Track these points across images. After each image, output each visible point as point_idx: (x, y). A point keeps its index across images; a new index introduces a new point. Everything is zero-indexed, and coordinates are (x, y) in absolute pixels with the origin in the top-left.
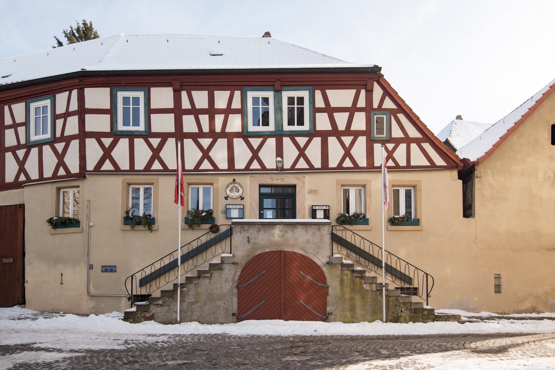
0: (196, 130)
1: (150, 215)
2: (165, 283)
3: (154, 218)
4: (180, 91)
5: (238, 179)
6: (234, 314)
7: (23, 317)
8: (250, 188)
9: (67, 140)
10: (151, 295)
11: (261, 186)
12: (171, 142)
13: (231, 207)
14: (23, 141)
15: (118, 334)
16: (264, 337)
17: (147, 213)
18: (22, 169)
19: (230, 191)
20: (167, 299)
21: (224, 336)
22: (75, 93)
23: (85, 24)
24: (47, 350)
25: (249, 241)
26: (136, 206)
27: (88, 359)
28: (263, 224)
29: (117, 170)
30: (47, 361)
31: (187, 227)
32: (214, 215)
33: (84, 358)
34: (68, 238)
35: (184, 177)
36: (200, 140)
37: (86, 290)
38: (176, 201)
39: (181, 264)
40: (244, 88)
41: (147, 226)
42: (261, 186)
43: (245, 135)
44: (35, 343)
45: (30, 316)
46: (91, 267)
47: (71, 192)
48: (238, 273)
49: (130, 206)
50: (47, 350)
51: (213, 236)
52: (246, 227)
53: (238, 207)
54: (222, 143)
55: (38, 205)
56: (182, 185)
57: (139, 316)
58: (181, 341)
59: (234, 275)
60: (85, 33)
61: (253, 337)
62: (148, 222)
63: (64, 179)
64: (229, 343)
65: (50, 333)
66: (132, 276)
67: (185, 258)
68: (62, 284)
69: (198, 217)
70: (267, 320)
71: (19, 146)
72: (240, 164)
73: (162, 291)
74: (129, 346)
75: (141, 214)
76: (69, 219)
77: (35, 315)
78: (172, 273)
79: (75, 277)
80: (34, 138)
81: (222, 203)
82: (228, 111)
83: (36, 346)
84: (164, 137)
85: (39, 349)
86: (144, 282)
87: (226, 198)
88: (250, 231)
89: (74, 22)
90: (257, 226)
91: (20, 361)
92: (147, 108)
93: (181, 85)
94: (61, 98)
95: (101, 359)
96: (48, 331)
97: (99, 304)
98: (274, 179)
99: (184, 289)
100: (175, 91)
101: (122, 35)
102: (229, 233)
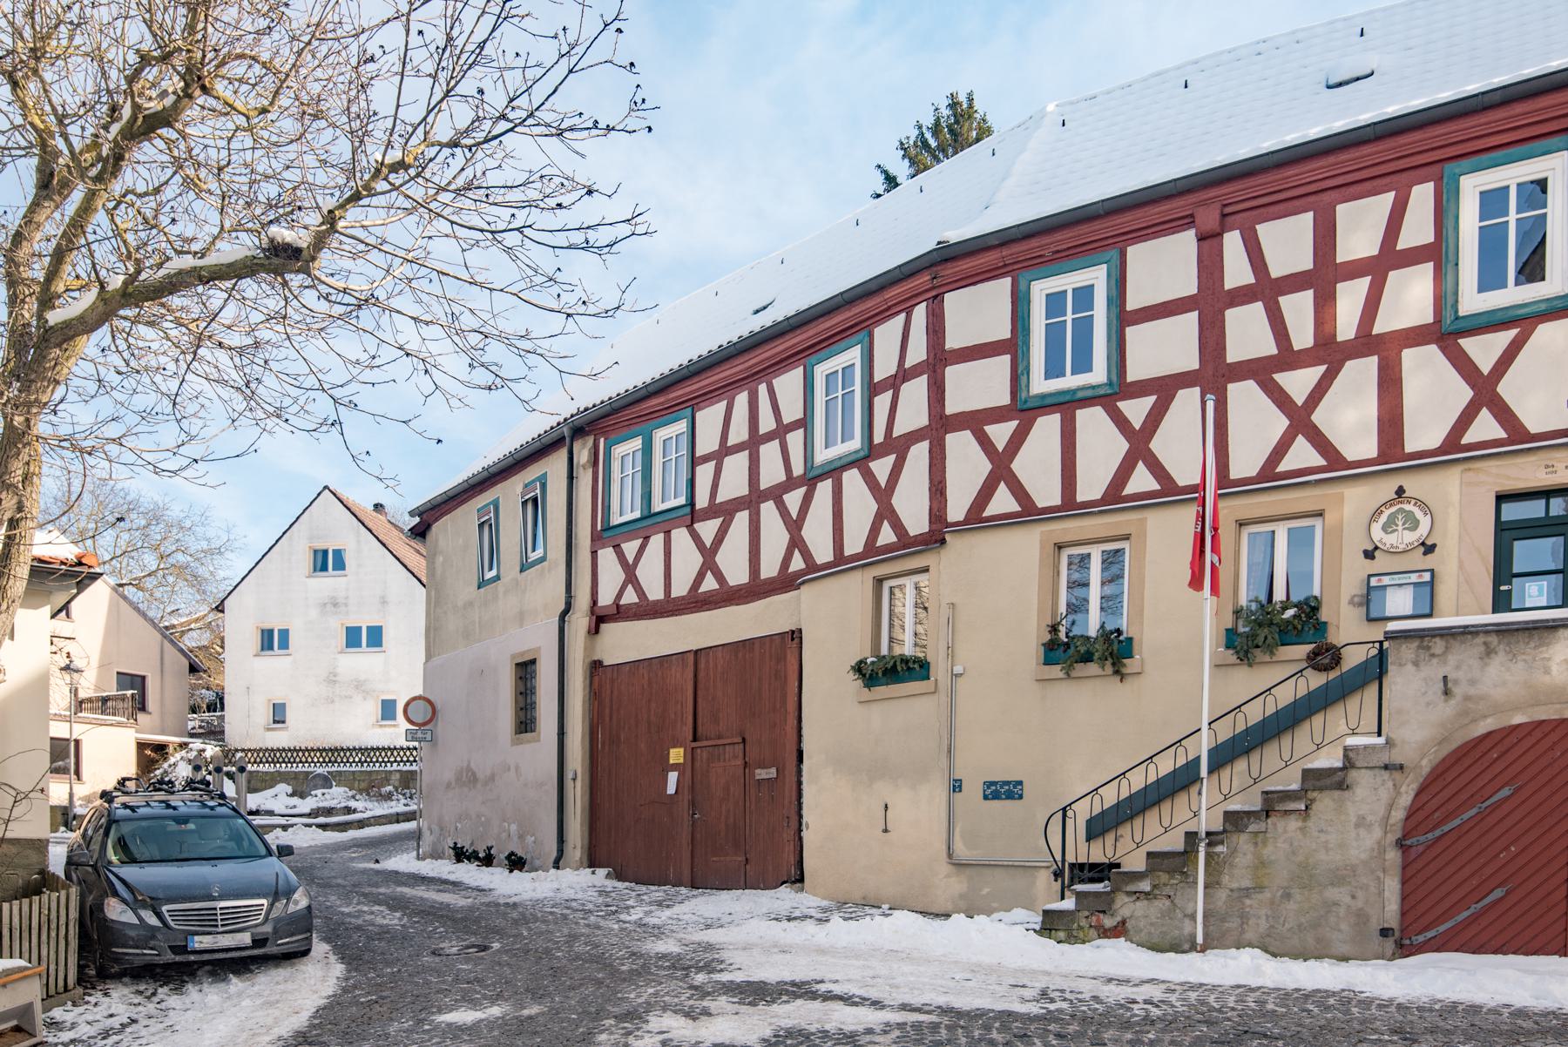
0: (1269, 348)
1: (1119, 632)
2: (1160, 832)
3: (1130, 640)
4: (1220, 235)
5: (1415, 485)
6: (1385, 932)
7: (797, 913)
8: (1459, 510)
9: (899, 447)
10: (1118, 866)
11: (1501, 498)
12: (1187, 401)
13: (1386, 580)
14: (798, 470)
15: (1023, 971)
16: (1495, 1011)
17: (1109, 627)
18: (797, 542)
19: (1385, 528)
20: (1164, 877)
21: (1346, 999)
22: (920, 313)
23: (954, 105)
24: (847, 999)
25: (1447, 692)
26: (1077, 607)
27: (943, 1032)
28: (1503, 631)
29: (1029, 512)
30: (848, 1028)
31: (1233, 659)
32: (1324, 615)
33: (935, 1027)
34: (905, 708)
35: (1221, 504)
36: (1282, 378)
37: (944, 847)
38: (1196, 582)
39: (1210, 772)
40: (1449, 168)
41: (1109, 663)
42: (1501, 498)
43: (1446, 333)
44: (822, 982)
45: (813, 912)
46: (957, 786)
47: (909, 582)
48: (1406, 799)
49: (1063, 609)
50: (847, 999)
51: (1316, 680)
52: (1438, 645)
53: (1414, 578)
54: (1362, 373)
55: (833, 625)
56: (1215, 529)
57: (1083, 923)
58: (1203, 1003)
59: (1391, 806)
60: (955, 131)
61: (1453, 1008)
62: (1114, 651)
63: (902, 550)
64: (1363, 1022)
65: (857, 957)
66: (1064, 810)
67: (1223, 756)
68: (886, 831)
69: (1271, 624)
70: (1511, 957)
71: (790, 483)
72: (1423, 434)
73: (1149, 854)
74: (1052, 1007)
75: (1093, 631)
76: (905, 660)
77: (824, 910)
78: (1181, 799)
79: (919, 811)
80: (822, 455)
81: (1354, 572)
82: (1390, 258)
83: (822, 988)
84: (1164, 389)
85: (829, 997)
86: (1098, 827)
87: (1369, 555)
88: (1452, 659)
89: (922, 111)
90: (1481, 639)
91: (787, 1023)
92: (1115, 310)
93: (1224, 216)
94: (887, 335)
95: (976, 1033)
96: (852, 953)
97: (975, 884)
98: (1560, 466)
99: (1219, 849)
100: (1201, 239)
101: (1051, 107)
102: (1376, 669)
